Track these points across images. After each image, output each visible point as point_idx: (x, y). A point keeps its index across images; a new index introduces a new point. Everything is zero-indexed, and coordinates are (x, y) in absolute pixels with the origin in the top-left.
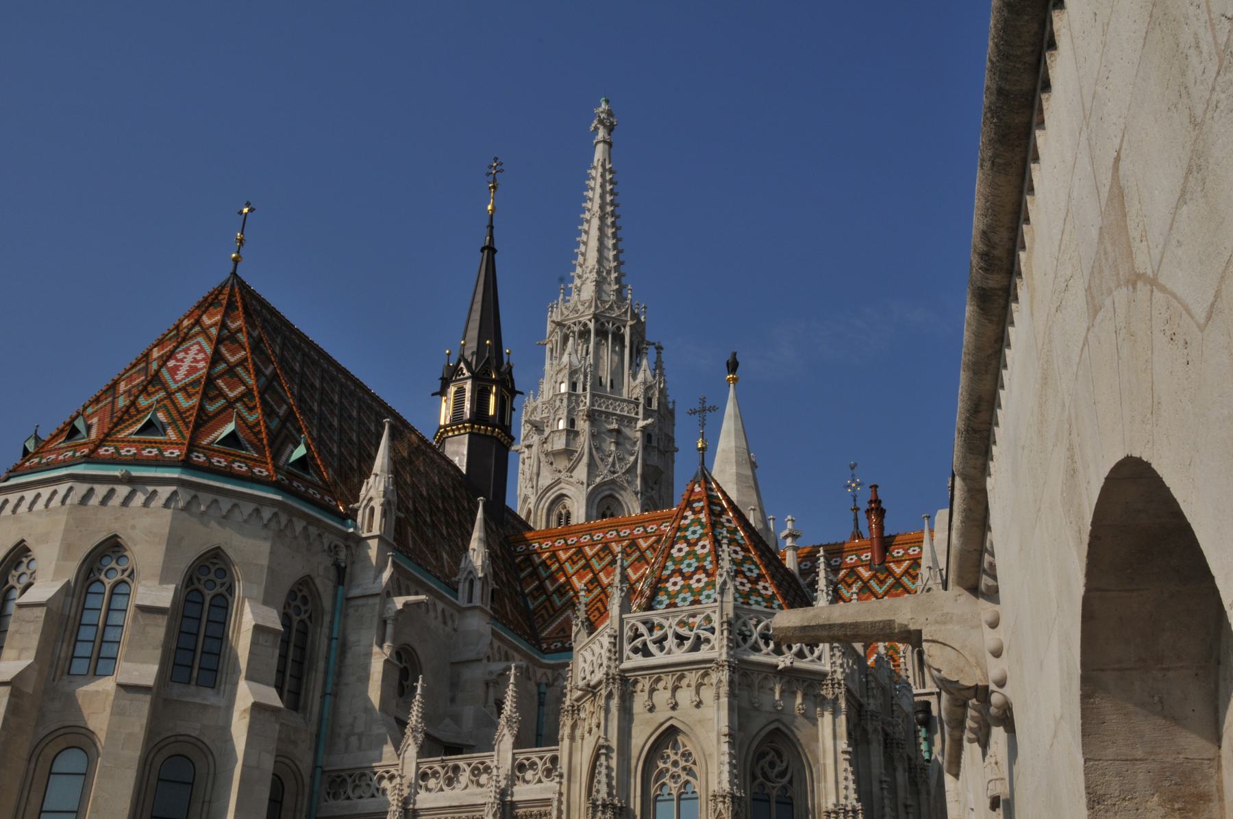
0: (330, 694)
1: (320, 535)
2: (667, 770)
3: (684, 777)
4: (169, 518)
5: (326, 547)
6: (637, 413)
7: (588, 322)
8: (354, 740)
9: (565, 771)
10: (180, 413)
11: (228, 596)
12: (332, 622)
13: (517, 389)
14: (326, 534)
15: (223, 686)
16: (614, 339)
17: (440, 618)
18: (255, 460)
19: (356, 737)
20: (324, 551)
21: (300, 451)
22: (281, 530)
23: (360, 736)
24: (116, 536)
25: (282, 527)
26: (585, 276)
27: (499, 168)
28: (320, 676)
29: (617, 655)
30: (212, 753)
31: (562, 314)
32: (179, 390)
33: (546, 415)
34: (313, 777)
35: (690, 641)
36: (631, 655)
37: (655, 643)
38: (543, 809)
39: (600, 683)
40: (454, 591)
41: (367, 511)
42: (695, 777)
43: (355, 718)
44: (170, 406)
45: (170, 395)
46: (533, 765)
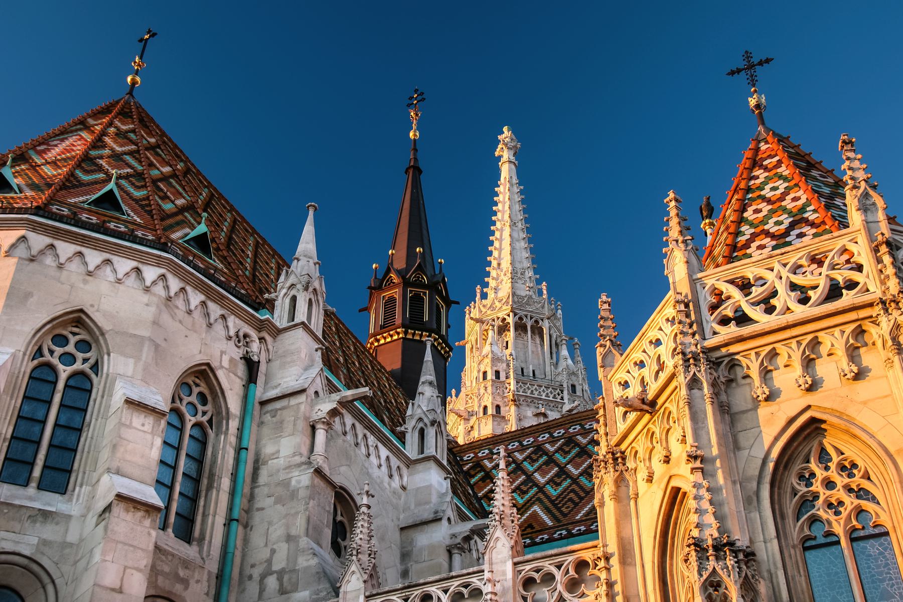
0: (237, 520)
1: (223, 317)
2: (816, 496)
3: (850, 502)
4: (12, 269)
5: (232, 333)
6: (562, 398)
8: (272, 582)
9: (613, 548)
11: (93, 376)
12: (241, 430)
14: (233, 317)
15: (77, 489)
16: (533, 332)
17: (384, 468)
18: (139, 225)
19: (275, 575)
20: (229, 338)
22: (169, 299)
23: (281, 574)
25: (172, 294)
26: (500, 278)
27: (420, 98)
28: (224, 498)
29: (695, 327)
30: (53, 582)
31: (480, 311)
33: (471, 405)
35: (820, 289)
36: (718, 328)
37: (757, 304)
40: (401, 437)
41: (287, 301)
42: (874, 499)
43: (273, 551)
46: (549, 578)
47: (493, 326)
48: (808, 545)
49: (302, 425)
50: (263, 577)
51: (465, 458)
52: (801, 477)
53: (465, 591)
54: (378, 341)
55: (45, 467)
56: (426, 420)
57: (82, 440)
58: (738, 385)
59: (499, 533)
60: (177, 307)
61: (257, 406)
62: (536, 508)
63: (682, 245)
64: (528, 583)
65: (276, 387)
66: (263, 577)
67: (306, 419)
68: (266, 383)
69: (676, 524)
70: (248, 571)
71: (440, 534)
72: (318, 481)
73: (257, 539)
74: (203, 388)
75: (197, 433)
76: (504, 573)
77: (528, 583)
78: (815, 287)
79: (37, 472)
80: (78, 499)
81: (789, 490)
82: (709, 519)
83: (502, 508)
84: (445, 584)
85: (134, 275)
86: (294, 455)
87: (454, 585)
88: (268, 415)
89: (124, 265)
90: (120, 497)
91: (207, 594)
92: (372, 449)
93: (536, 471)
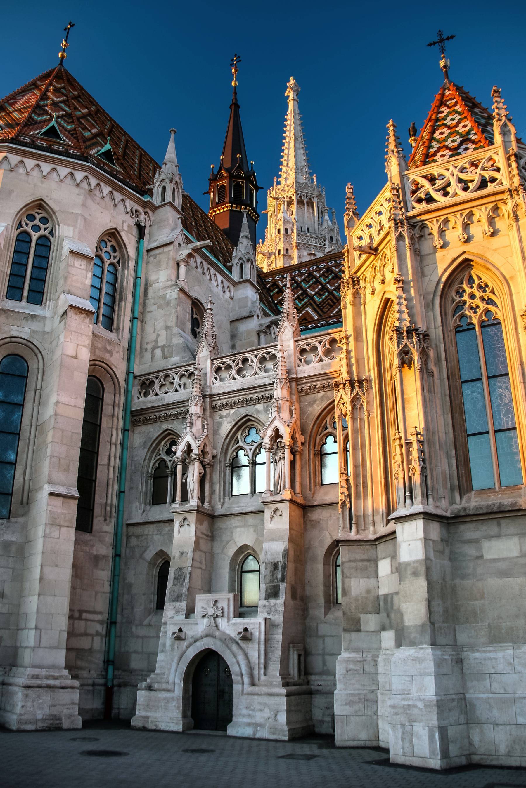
1: (123, 200)
2: (465, 303)
3: (482, 306)
5: (128, 209)
6: (325, 245)
8: (158, 352)
9: (350, 332)
11: (51, 238)
12: (136, 266)
14: (128, 200)
15: (48, 302)
16: (308, 205)
17: (220, 287)
18: (70, 146)
20: (127, 213)
22: (91, 190)
23: (163, 348)
25: (92, 188)
27: (238, 60)
29: (402, 204)
30: (41, 352)
31: (276, 192)
34: (127, 380)
35: (475, 183)
36: (415, 205)
38: (326, 382)
40: (230, 269)
41: (160, 189)
42: (495, 305)
43: (158, 335)
47: (284, 201)
48: (458, 330)
49: (172, 264)
50: (153, 349)
51: (268, 280)
52: (457, 292)
54: (215, 211)
55: (29, 290)
56: (244, 259)
57: (48, 275)
58: (426, 239)
59: (286, 324)
60: (96, 195)
62: (308, 309)
63: (396, 154)
64: (303, 351)
65: (155, 241)
66: (153, 349)
67: (174, 259)
68: (150, 239)
69: (386, 318)
70: (145, 346)
71: (253, 324)
72: (182, 295)
73: (149, 329)
74: (113, 243)
75: (111, 269)
76: (289, 346)
77: (303, 351)
78: (472, 181)
79: (25, 293)
80: (49, 308)
81: (450, 299)
82: (405, 316)
83: (288, 310)
84: (255, 353)
85: (69, 177)
86: (168, 280)
87: (261, 353)
88: (152, 258)
89: (64, 171)
90: (71, 306)
91: (123, 359)
92: (213, 276)
93: (308, 288)
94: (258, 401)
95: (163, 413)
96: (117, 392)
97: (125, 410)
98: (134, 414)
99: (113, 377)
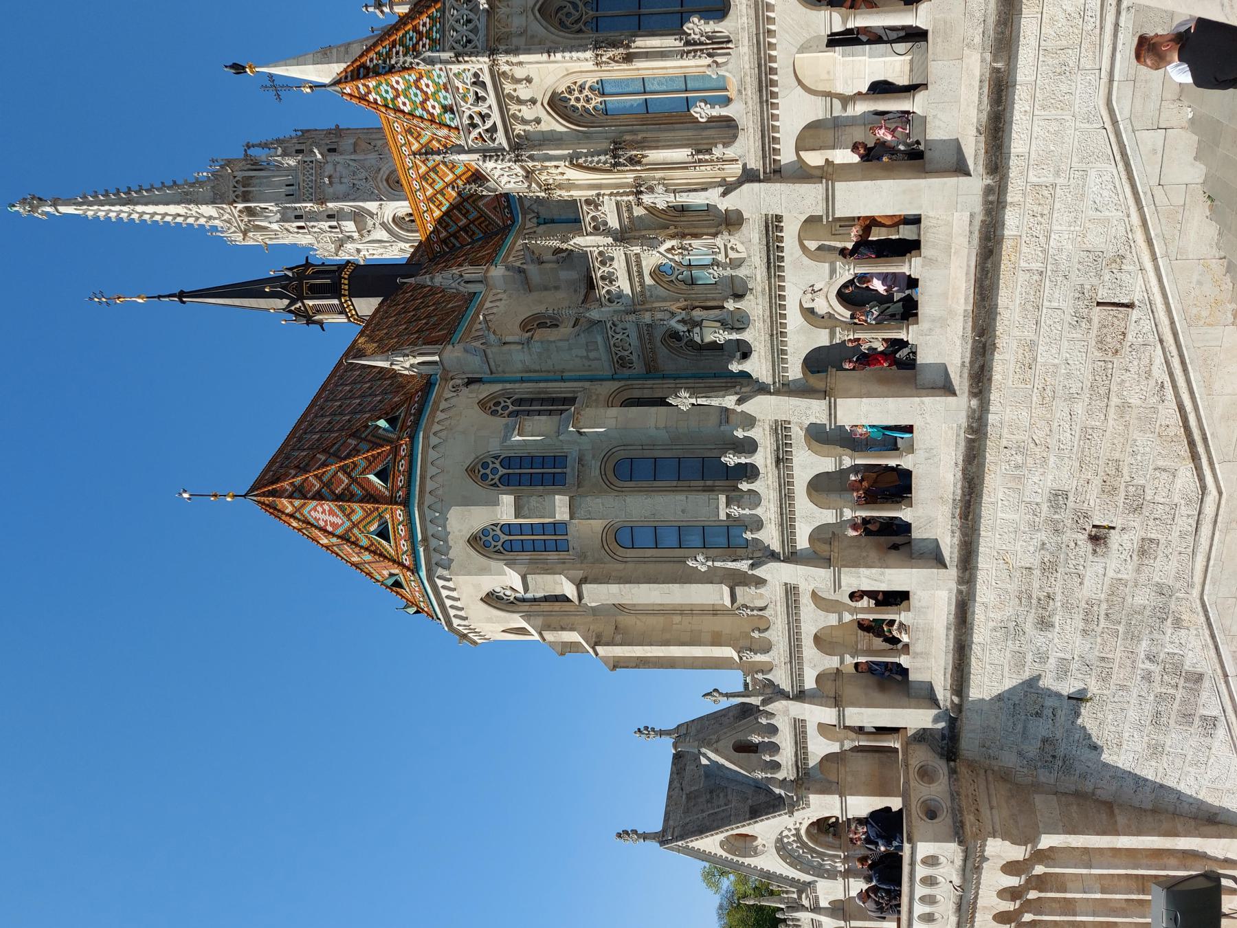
1: (446, 400)
5: (455, 394)
6: (312, 162)
7: (238, 209)
8: (592, 355)
9: (594, 192)
10: (368, 515)
12: (510, 382)
13: (304, 262)
17: (498, 304)
21: (382, 423)
23: (587, 351)
24: (468, 541)
28: (550, 385)
32: (350, 519)
34: (619, 380)
35: (478, 90)
37: (484, 122)
39: (522, 167)
44: (364, 523)
45: (355, 525)
47: (249, 221)
49: (506, 348)
53: (599, 259)
54: (352, 315)
56: (459, 280)
61: (494, 375)
62: (480, 204)
63: (447, 155)
79: (559, 470)
82: (603, 158)
94: (639, 265)
95: (648, 346)
96: (631, 387)
97: (646, 379)
98: (648, 371)
99: (619, 391)
